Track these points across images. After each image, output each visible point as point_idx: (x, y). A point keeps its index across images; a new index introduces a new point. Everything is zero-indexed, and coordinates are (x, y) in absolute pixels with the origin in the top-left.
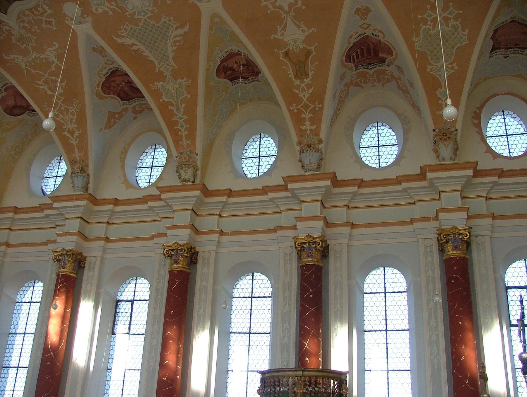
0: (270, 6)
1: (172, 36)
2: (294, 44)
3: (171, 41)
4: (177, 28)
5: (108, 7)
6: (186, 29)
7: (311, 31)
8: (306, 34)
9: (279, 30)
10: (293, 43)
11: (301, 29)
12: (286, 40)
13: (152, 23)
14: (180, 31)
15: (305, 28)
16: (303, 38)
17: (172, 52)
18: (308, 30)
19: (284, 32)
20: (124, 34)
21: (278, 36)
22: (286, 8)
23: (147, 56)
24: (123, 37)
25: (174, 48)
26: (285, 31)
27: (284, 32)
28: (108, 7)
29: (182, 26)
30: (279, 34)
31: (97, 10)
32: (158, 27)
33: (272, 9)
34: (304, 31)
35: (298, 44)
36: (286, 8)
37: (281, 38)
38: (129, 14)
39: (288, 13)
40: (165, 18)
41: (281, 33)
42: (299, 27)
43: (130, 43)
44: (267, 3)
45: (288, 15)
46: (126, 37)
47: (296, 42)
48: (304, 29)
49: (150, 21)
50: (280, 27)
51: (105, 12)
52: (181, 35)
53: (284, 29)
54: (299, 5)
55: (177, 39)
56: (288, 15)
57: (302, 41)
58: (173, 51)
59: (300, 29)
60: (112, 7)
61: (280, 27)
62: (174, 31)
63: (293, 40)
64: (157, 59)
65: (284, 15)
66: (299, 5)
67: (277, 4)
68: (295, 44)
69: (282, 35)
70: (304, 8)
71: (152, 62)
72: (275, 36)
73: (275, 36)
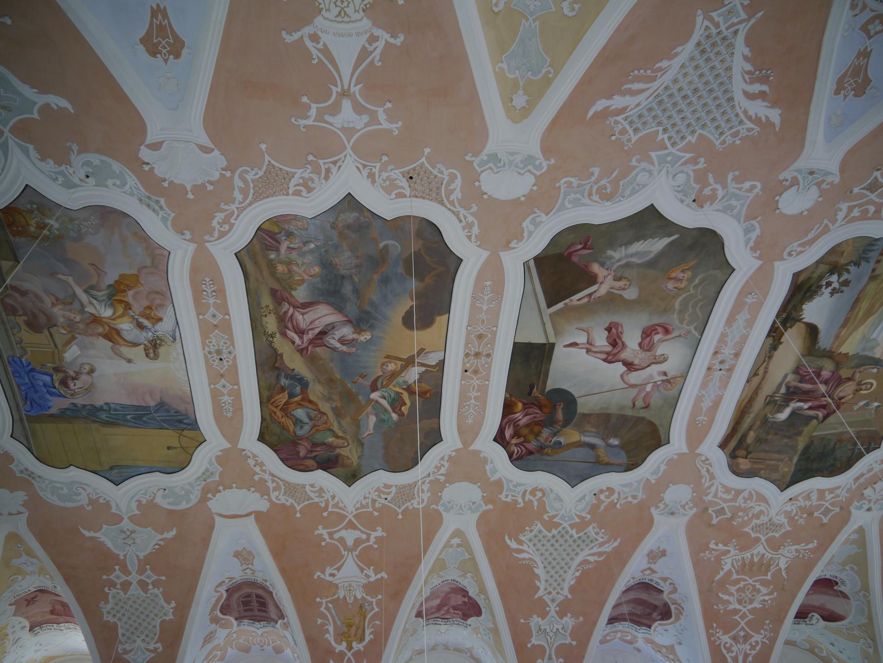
0: (382, 116)
1: (647, 94)
2: (345, 9)
3: (655, 85)
4: (623, 110)
5: (725, 186)
6: (601, 104)
7: (296, 36)
8: (307, 30)
9: (377, 54)
10: (350, 11)
11: (320, 46)
12: (366, 23)
13: (666, 136)
14: (618, 102)
15: (309, 44)
16: (319, 21)
17: (677, 54)
18: (302, 37)
19: (367, 46)
20: (749, 125)
21: (384, 36)
22: (346, 104)
23: (746, 58)
24: (757, 120)
25: (664, 64)
26: (364, 48)
27: (367, 46)
28: (725, 186)
29: (606, 113)
30: (381, 44)
31: (753, 187)
32: (659, 124)
33: (380, 110)
34: (315, 38)
35: (336, 6)
36: (346, 104)
37: (378, 32)
38: (697, 163)
39: (345, 94)
40: (629, 140)
41: (375, 45)
42: (326, 51)
43: (759, 102)
44: (385, 125)
45: (346, 87)
46: (749, 118)
47: (340, 13)
48: (315, 44)
49: (666, 140)
50: (372, 61)
51: (738, 180)
52: (624, 93)
53: (364, 54)
54: (314, 106)
55: (636, 86)
56: (346, 87)
57: (323, 12)
58: (671, 57)
59: (325, 45)
60: (718, 187)
61: (372, 61)
62: (633, 106)
63: (346, 19)
64: (731, 46)
65: (356, 89)
66: (314, 106)
67: (365, 118)
68: (342, 9)
69: (373, 39)
70: (305, 99)
71: (748, 42)
72: (392, 40)
73: (392, 40)
